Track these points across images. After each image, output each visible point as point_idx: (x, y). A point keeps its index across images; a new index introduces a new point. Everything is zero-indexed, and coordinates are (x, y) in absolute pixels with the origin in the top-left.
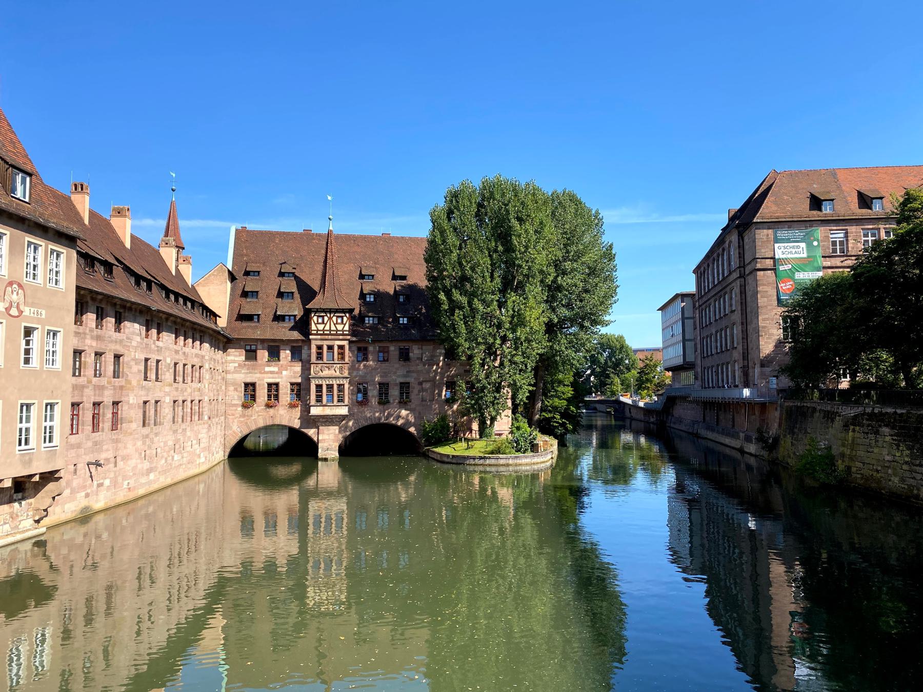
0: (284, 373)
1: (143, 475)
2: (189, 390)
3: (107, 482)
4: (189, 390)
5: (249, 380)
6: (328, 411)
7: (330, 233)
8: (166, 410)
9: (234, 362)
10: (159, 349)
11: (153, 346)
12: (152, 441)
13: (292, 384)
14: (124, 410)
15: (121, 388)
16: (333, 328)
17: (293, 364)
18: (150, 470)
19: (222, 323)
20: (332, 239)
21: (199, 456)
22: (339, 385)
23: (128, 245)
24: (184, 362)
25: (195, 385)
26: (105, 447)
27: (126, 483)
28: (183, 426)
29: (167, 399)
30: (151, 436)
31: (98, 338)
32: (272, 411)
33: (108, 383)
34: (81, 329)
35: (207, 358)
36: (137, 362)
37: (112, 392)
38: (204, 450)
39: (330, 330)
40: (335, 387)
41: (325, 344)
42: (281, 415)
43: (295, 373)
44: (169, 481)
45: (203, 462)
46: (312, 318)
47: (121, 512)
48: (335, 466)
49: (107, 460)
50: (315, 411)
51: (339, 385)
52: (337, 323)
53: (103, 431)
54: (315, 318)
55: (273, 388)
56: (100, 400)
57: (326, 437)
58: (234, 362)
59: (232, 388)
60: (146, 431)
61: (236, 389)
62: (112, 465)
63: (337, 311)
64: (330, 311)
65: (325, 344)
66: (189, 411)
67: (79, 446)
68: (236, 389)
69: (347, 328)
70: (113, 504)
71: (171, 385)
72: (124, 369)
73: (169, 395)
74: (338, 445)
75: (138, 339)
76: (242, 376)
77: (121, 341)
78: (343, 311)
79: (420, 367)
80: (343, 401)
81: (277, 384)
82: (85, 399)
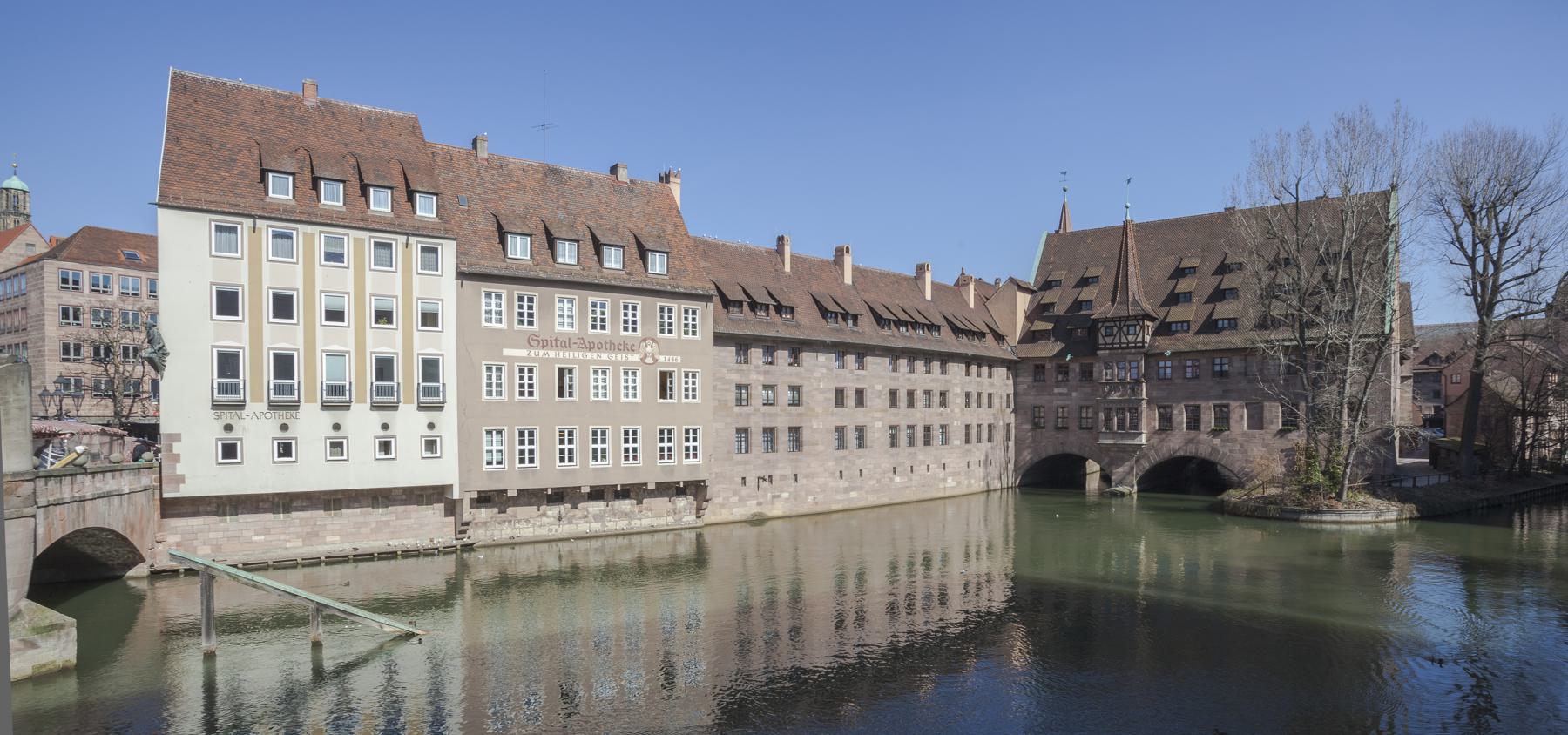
1: (837, 492)
2: (919, 415)
10: (859, 378)
11: (849, 376)
18: (847, 490)
20: (1131, 233)
21: (945, 480)
27: (810, 499)
29: (879, 424)
31: (766, 373)
34: (744, 366)
36: (822, 391)
38: (954, 474)
44: (885, 500)
45: (951, 485)
49: (784, 477)
63: (1128, 318)
67: (747, 463)
72: (805, 398)
73: (880, 419)
82: (752, 425)
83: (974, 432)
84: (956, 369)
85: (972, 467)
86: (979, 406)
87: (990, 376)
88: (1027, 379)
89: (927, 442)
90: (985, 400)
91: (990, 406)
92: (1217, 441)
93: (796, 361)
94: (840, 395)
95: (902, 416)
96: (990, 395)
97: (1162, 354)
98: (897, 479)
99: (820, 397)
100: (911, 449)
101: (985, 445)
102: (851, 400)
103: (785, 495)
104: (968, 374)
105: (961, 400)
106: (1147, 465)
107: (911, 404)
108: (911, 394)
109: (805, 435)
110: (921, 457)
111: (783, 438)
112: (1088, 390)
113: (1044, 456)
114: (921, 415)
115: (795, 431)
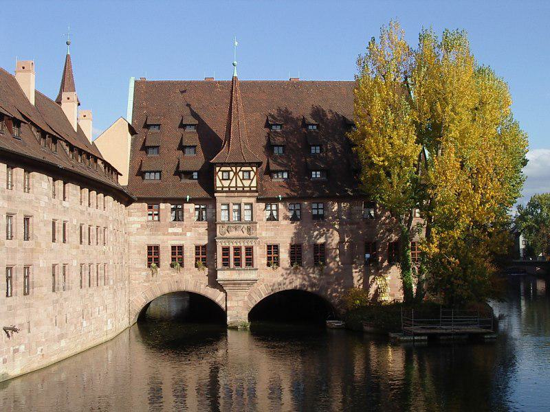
0: (189, 234)
3: (22, 348)
4: (94, 253)
5: (153, 242)
7: (234, 79)
8: (74, 275)
9: (134, 223)
10: (66, 210)
12: (61, 305)
14: (35, 275)
15: (32, 250)
16: (240, 184)
18: (61, 337)
19: (123, 181)
20: (237, 86)
23: (32, 102)
24: (89, 223)
25: (101, 247)
27: (39, 349)
28: (91, 291)
29: (75, 263)
30: (61, 301)
31: (9, 199)
33: (20, 245)
35: (111, 218)
39: (236, 187)
40: (243, 250)
44: (79, 349)
49: (21, 325)
52: (243, 179)
54: (220, 174)
55: (178, 251)
57: (235, 304)
58: (134, 223)
60: (55, 296)
61: (139, 253)
62: (27, 331)
64: (236, 165)
66: (92, 277)
68: (139, 253)
69: (254, 184)
74: (247, 312)
76: (145, 237)
77: (30, 201)
78: (250, 164)
81: (181, 248)
106: (259, 300)
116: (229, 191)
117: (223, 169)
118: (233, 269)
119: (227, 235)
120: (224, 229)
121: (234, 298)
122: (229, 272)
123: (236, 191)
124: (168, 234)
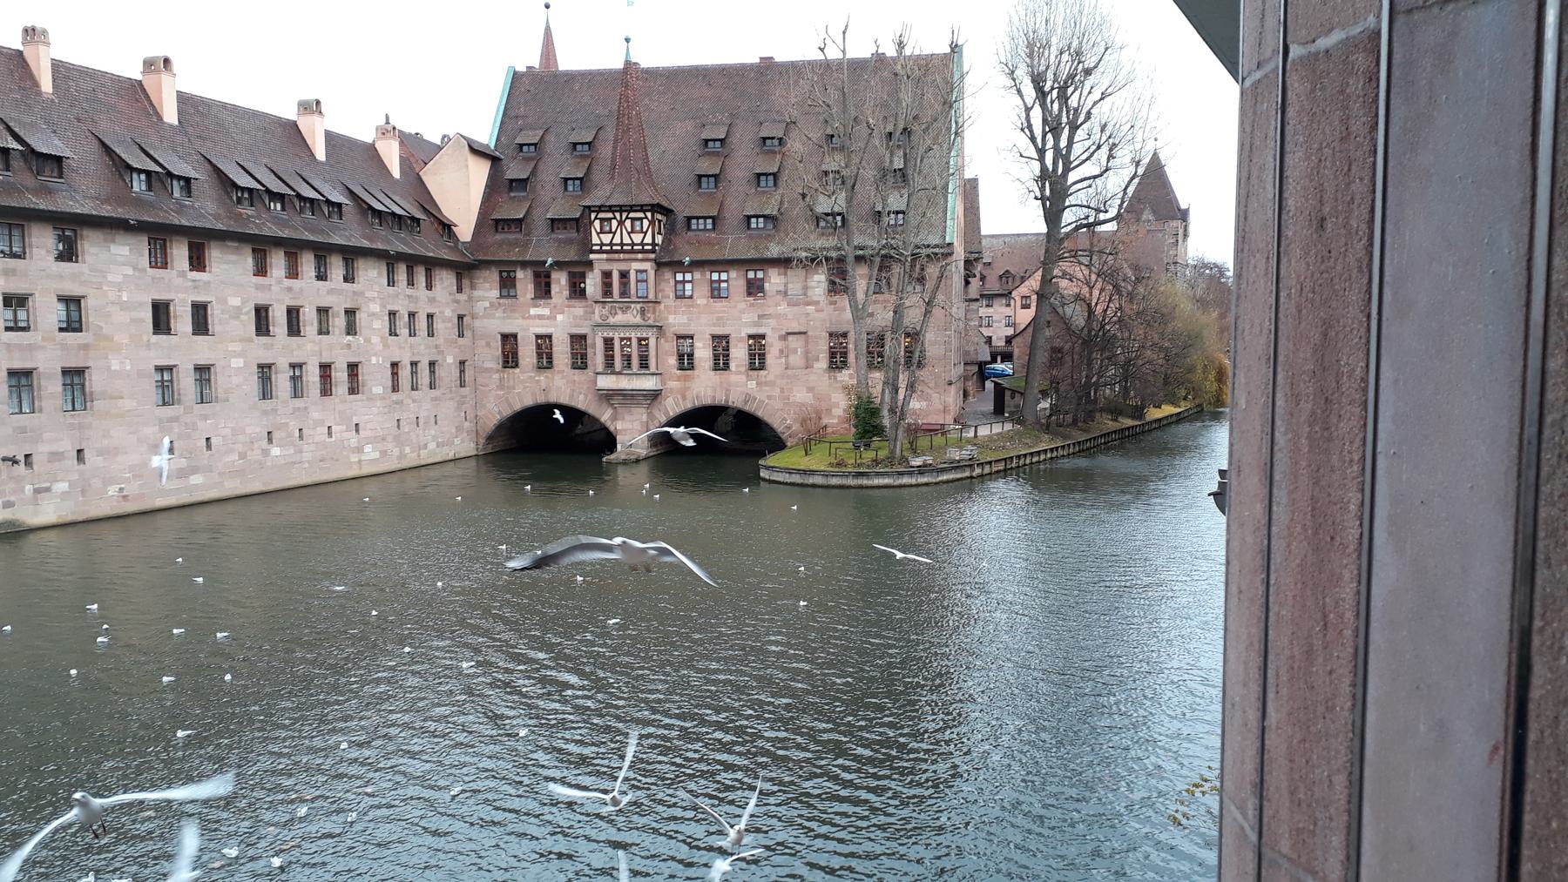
0: (560, 317)
4: (311, 348)
5: (507, 330)
6: (624, 383)
13: (572, 336)
15: (86, 347)
16: (627, 240)
17: (573, 302)
21: (359, 450)
22: (640, 340)
26: (46, 436)
27: (113, 490)
32: (542, 378)
36: (124, 306)
37: (59, 353)
39: (622, 244)
41: (615, 269)
42: (559, 388)
43: (575, 317)
45: (370, 458)
46: (591, 223)
47: (110, 533)
48: (643, 469)
49: (56, 456)
50: (606, 382)
51: (640, 340)
52: (633, 231)
53: (40, 411)
54: (597, 223)
55: (544, 344)
56: (28, 365)
57: (628, 426)
59: (483, 343)
61: (488, 344)
65: (615, 269)
69: (648, 239)
70: (80, 519)
71: (251, 340)
73: (239, 355)
75: (129, 271)
78: (642, 208)
79: (783, 308)
80: (647, 367)
83: (405, 373)
84: (371, 275)
85: (405, 428)
86: (412, 334)
87: (429, 287)
88: (487, 289)
89: (326, 390)
90: (422, 323)
91: (431, 334)
92: (752, 384)
93: (68, 254)
94: (161, 317)
95: (280, 348)
96: (430, 316)
97: (681, 263)
98: (276, 451)
99: (121, 317)
100: (298, 403)
101: (424, 392)
102: (182, 321)
103: (61, 486)
104: (391, 282)
105: (381, 324)
107: (294, 328)
108: (293, 314)
109: (95, 381)
110: (315, 415)
111: (51, 388)
112: (578, 309)
113: (518, 407)
114: (311, 348)
115: (74, 376)
116: (612, 252)
117: (601, 215)
118: (619, 373)
119: (612, 320)
120: (605, 311)
121: (627, 417)
122: (613, 378)
123: (622, 251)
124: (530, 317)
